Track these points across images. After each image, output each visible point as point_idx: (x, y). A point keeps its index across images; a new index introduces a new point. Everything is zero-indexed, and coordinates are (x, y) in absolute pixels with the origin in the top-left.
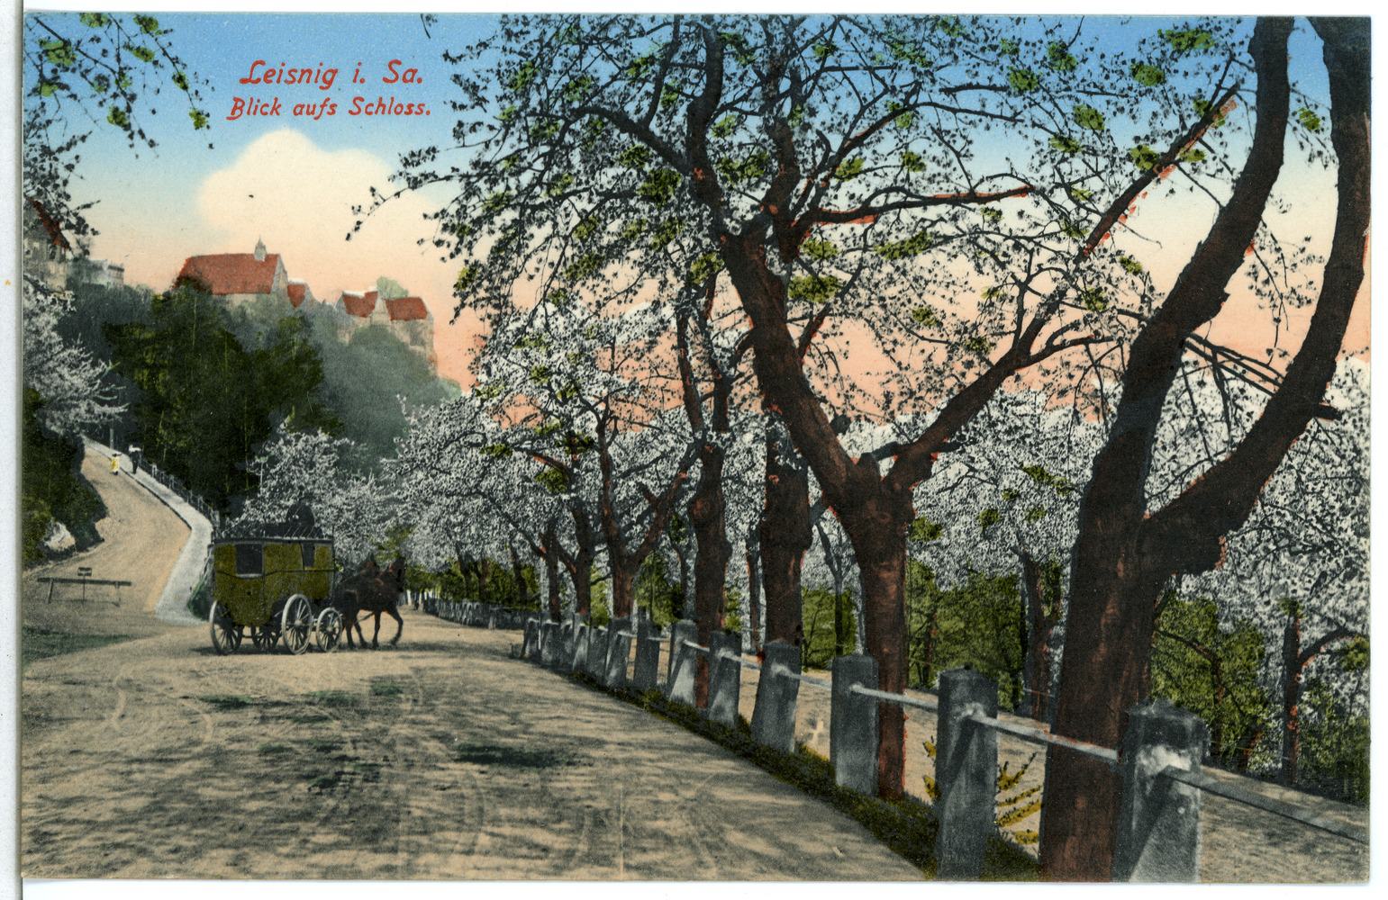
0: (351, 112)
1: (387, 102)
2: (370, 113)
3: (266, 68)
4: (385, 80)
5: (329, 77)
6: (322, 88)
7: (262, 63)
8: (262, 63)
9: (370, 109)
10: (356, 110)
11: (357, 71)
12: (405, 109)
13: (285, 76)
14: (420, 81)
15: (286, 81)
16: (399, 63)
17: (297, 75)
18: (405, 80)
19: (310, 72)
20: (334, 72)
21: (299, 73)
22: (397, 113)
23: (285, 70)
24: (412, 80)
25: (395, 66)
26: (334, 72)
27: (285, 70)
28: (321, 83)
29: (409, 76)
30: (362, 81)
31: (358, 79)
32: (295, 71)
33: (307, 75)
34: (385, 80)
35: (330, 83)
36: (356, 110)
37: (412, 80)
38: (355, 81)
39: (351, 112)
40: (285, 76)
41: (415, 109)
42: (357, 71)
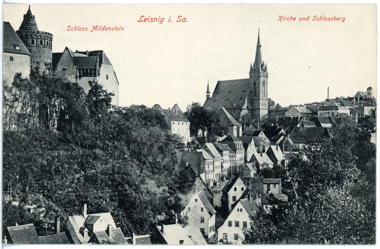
2: (318, 20)
3: (145, 17)
4: (177, 21)
5: (162, 21)
6: (160, 23)
7: (144, 16)
8: (144, 16)
9: (318, 19)
10: (314, 19)
11: (170, 19)
12: (328, 19)
13: (150, 20)
15: (150, 21)
16: (181, 16)
17: (153, 20)
18: (183, 22)
19: (157, 19)
20: (163, 19)
21: (154, 19)
23: (150, 18)
24: (184, 21)
25: (180, 17)
26: (163, 19)
27: (150, 18)
29: (184, 20)
30: (171, 21)
31: (170, 21)
32: (153, 19)
33: (156, 20)
34: (177, 21)
35: (162, 22)
36: (314, 19)
37: (184, 21)
38: (169, 21)
40: (150, 20)
41: (331, 19)
42: (170, 19)
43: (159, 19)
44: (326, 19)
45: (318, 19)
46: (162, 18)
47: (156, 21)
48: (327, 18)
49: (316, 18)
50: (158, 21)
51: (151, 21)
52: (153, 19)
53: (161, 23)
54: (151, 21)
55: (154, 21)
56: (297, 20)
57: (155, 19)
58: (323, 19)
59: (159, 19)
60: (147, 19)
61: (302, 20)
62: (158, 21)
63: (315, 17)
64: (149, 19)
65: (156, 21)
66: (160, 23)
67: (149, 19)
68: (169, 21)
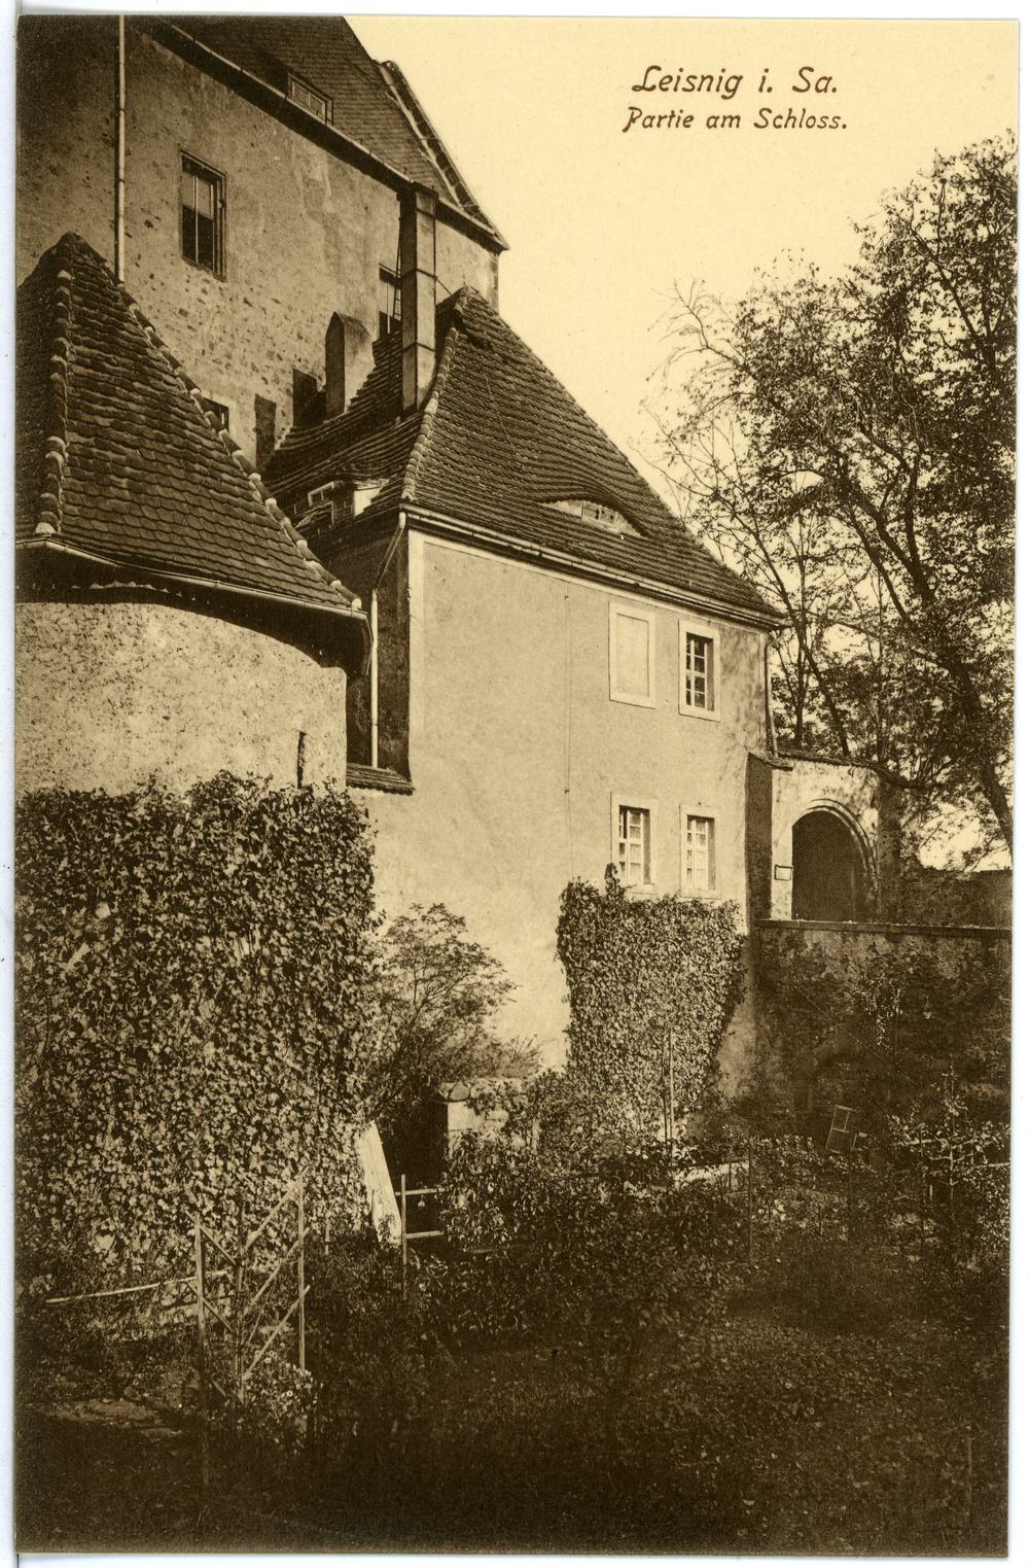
0: (756, 125)
1: (797, 113)
4: (795, 89)
5: (731, 86)
6: (724, 97)
7: (658, 68)
8: (658, 68)
9: (778, 122)
10: (763, 123)
11: (764, 78)
12: (818, 122)
13: (683, 84)
14: (834, 90)
15: (685, 90)
16: (811, 70)
17: (697, 83)
19: (711, 78)
20: (739, 79)
21: (699, 80)
22: (809, 127)
23: (684, 76)
24: (825, 90)
25: (806, 73)
26: (739, 79)
27: (684, 76)
28: (723, 90)
29: (822, 85)
30: (770, 90)
31: (765, 88)
32: (695, 78)
33: (708, 81)
34: (795, 89)
35: (735, 90)
36: (763, 123)
37: (825, 90)
38: (761, 90)
39: (756, 125)
40: (683, 84)
41: (829, 122)
42: (764, 78)
43: (721, 78)
44: (811, 122)
45: (778, 122)
46: (735, 77)
47: (709, 89)
48: (813, 118)
49: (770, 117)
50: (718, 90)
51: (690, 87)
52: (695, 78)
53: (728, 94)
54: (690, 87)
55: (699, 89)
56: (699, 124)
57: (703, 78)
58: (797, 124)
59: (721, 78)
60: (671, 78)
61: (728, 120)
62: (718, 90)
63: (765, 113)
64: (679, 78)
65: (709, 89)
66: (724, 97)
67: (679, 78)
68: (761, 90)
